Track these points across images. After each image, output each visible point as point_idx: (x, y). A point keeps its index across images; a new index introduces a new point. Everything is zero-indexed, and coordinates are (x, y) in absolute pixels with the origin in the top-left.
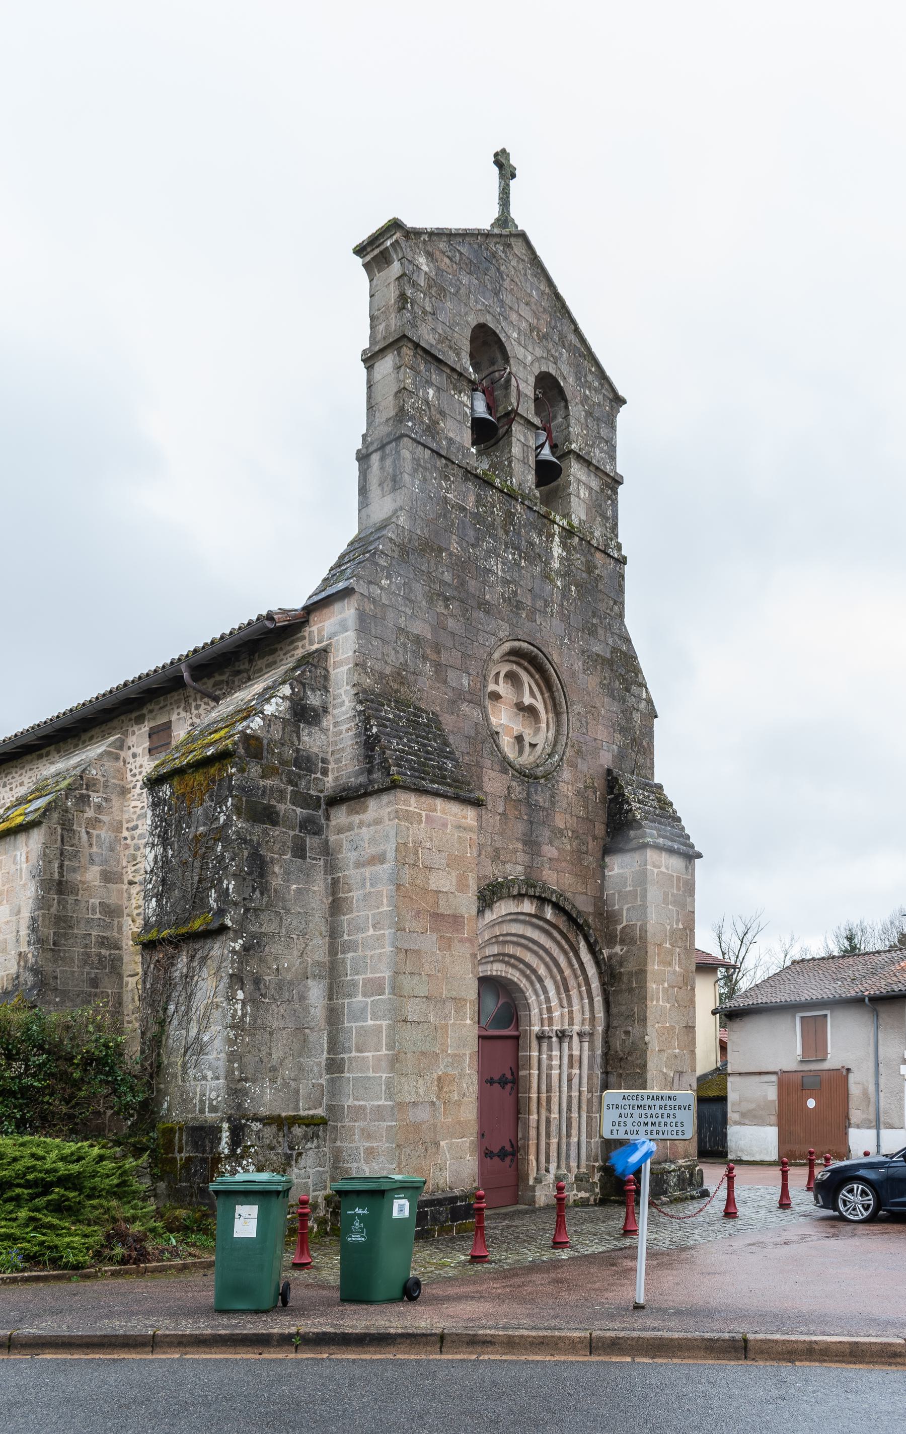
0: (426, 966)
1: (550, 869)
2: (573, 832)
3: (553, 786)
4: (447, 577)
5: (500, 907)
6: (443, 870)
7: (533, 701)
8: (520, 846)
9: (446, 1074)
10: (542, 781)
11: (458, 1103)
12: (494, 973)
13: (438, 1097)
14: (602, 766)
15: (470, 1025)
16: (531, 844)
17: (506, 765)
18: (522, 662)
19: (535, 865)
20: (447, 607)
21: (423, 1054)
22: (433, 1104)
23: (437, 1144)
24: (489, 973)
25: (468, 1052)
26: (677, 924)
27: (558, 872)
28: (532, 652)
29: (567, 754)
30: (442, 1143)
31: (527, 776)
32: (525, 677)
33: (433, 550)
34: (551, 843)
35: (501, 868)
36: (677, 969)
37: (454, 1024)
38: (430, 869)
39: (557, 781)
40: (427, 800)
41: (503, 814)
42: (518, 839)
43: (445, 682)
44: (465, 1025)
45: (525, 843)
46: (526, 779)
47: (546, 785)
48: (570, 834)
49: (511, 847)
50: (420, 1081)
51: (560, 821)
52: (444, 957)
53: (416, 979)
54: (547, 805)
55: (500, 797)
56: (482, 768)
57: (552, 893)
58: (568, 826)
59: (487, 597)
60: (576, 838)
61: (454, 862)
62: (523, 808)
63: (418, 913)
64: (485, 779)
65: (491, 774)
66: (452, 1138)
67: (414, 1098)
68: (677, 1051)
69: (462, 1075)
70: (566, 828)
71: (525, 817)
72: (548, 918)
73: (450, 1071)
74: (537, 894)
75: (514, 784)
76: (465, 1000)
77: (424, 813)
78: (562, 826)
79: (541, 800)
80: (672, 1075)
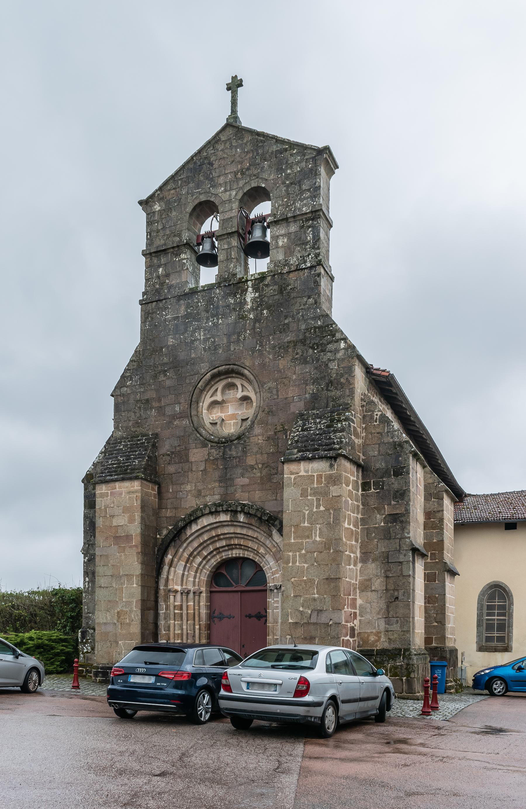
0: (111, 561)
1: (242, 492)
2: (263, 464)
3: (245, 441)
4: (166, 360)
5: (202, 521)
6: (120, 515)
7: (245, 393)
8: (217, 484)
9: (122, 611)
10: (236, 442)
11: (129, 624)
12: (234, 555)
13: (118, 621)
14: (294, 413)
15: (136, 587)
16: (226, 480)
17: (205, 442)
18: (231, 375)
19: (228, 492)
20: (166, 375)
21: (109, 601)
22: (115, 624)
23: (117, 643)
24: (230, 556)
25: (135, 600)
26: (318, 506)
27: (249, 492)
28: (228, 369)
29: (259, 417)
30: (120, 642)
31: (226, 443)
32: (238, 382)
33: (157, 351)
34: (243, 476)
35: (202, 500)
36: (318, 539)
37: (127, 587)
38: (112, 516)
39: (248, 438)
40: (112, 485)
41: (205, 471)
42: (214, 481)
43: (164, 415)
44: (133, 587)
45: (220, 481)
46: (222, 445)
47: (239, 443)
48: (260, 466)
49: (210, 486)
50: (108, 613)
51: (250, 461)
52: (121, 556)
53: (106, 568)
54: (239, 454)
55: (202, 461)
56: (189, 450)
57: (237, 506)
58: (258, 462)
59: (193, 356)
60: (266, 467)
61: (126, 510)
62: (219, 462)
63: (107, 538)
64: (191, 455)
65: (195, 451)
66: (125, 640)
67: (105, 621)
68: (316, 596)
69: (131, 611)
70: (257, 464)
71: (221, 467)
72: (242, 520)
73: (124, 609)
74: (225, 509)
75: (213, 450)
76: (133, 575)
77: (109, 492)
78: (253, 463)
79: (234, 453)
80: (310, 612)
